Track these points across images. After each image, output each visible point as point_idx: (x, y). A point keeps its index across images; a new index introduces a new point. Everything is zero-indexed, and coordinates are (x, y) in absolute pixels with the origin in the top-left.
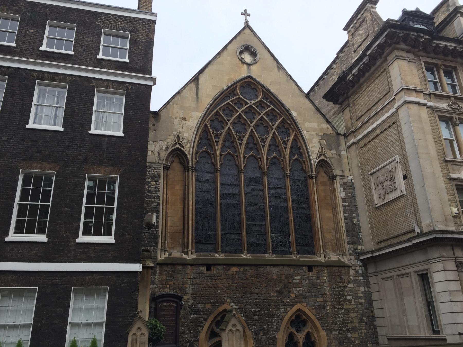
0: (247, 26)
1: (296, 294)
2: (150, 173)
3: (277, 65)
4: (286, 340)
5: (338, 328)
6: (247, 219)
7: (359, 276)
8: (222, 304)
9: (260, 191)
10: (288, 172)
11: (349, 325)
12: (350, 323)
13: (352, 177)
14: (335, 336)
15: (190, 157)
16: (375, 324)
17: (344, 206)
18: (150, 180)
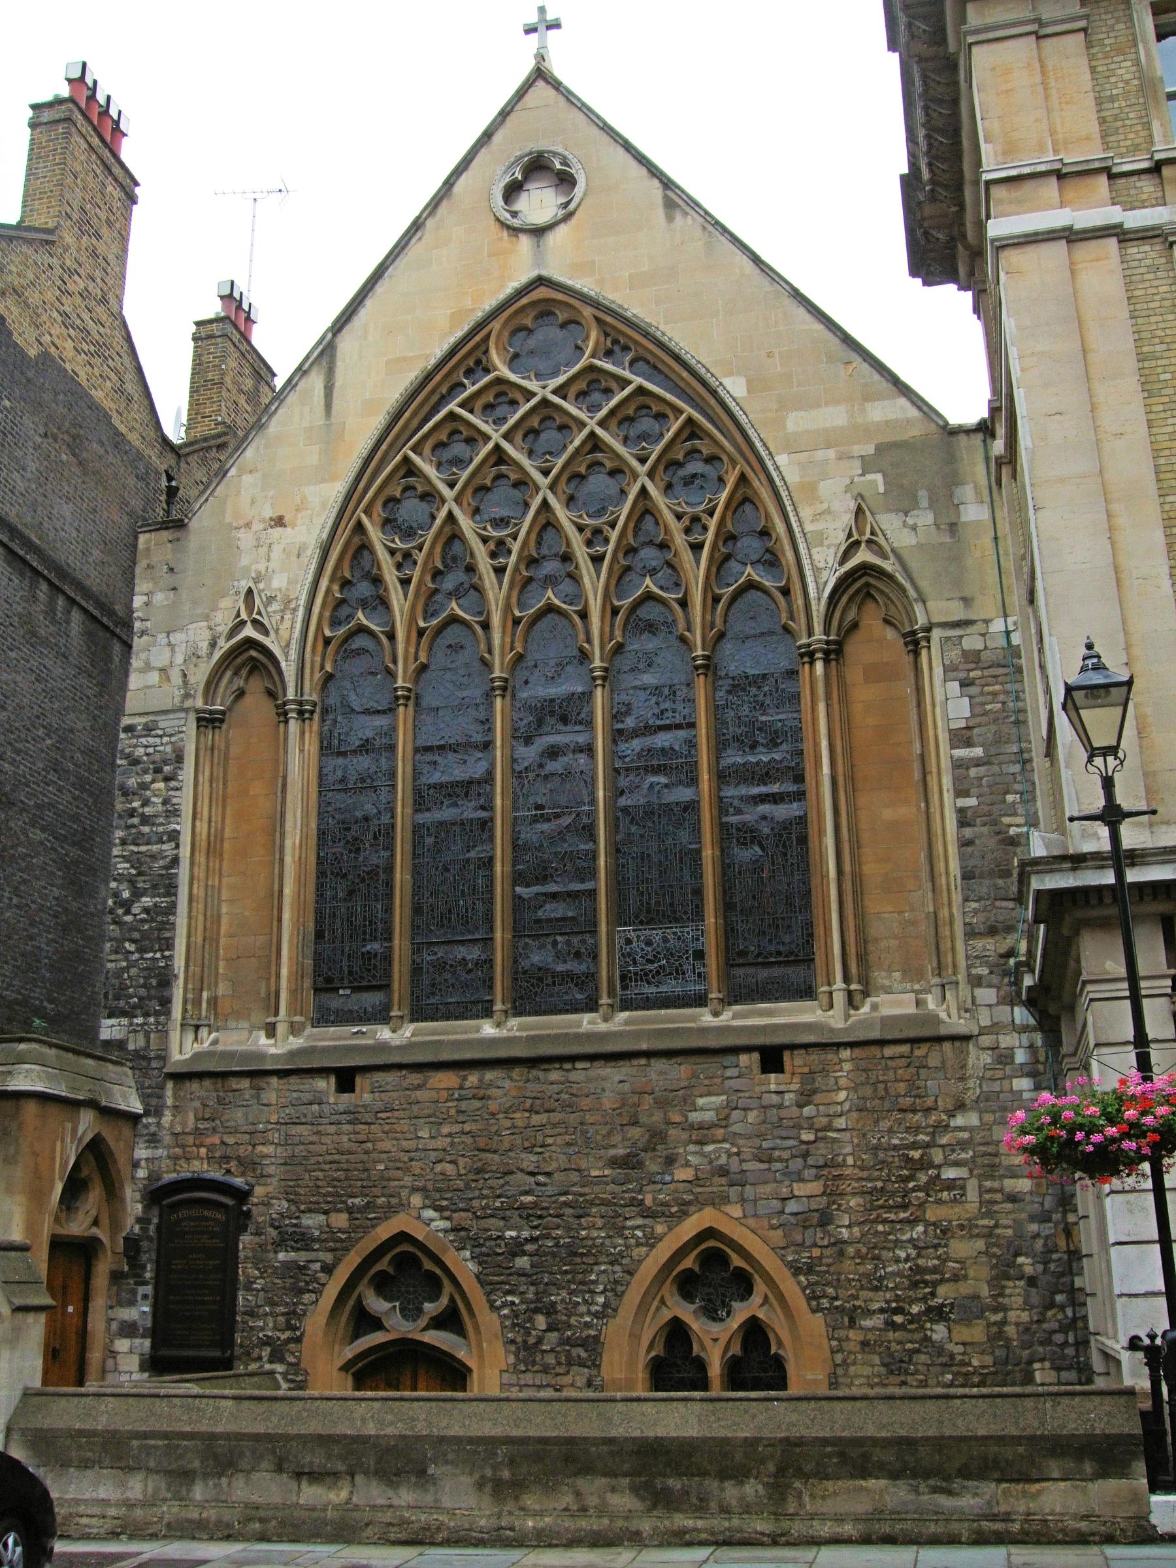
0: (540, 75)
1: (697, 1170)
2: (151, 750)
3: (666, 197)
4: (651, 1347)
5: (887, 1302)
6: (518, 878)
7: (1011, 1077)
8: (390, 1211)
9: (581, 751)
10: (699, 652)
11: (942, 1290)
12: (948, 1280)
13: (1010, 620)
14: (870, 1336)
15: (289, 668)
16: (1078, 1282)
17: (959, 765)
18: (148, 778)
